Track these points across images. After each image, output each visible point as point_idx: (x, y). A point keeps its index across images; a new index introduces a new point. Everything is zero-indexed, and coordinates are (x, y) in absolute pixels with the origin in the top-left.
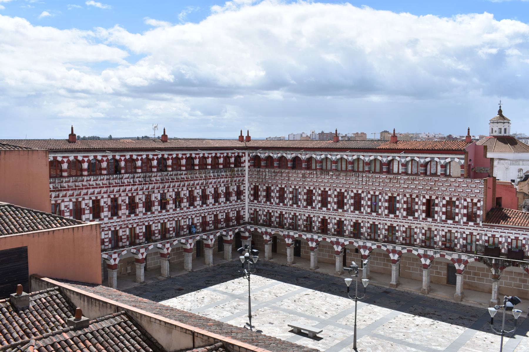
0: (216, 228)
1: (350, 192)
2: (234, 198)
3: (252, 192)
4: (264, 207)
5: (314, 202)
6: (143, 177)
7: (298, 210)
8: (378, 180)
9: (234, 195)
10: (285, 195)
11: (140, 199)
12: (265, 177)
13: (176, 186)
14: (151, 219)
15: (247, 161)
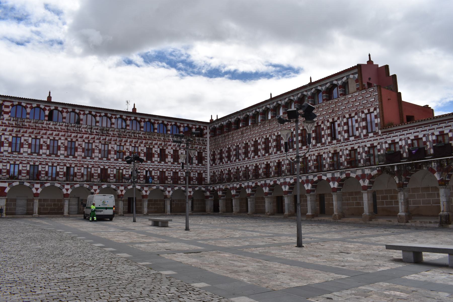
6: (101, 130)
15: (208, 133)
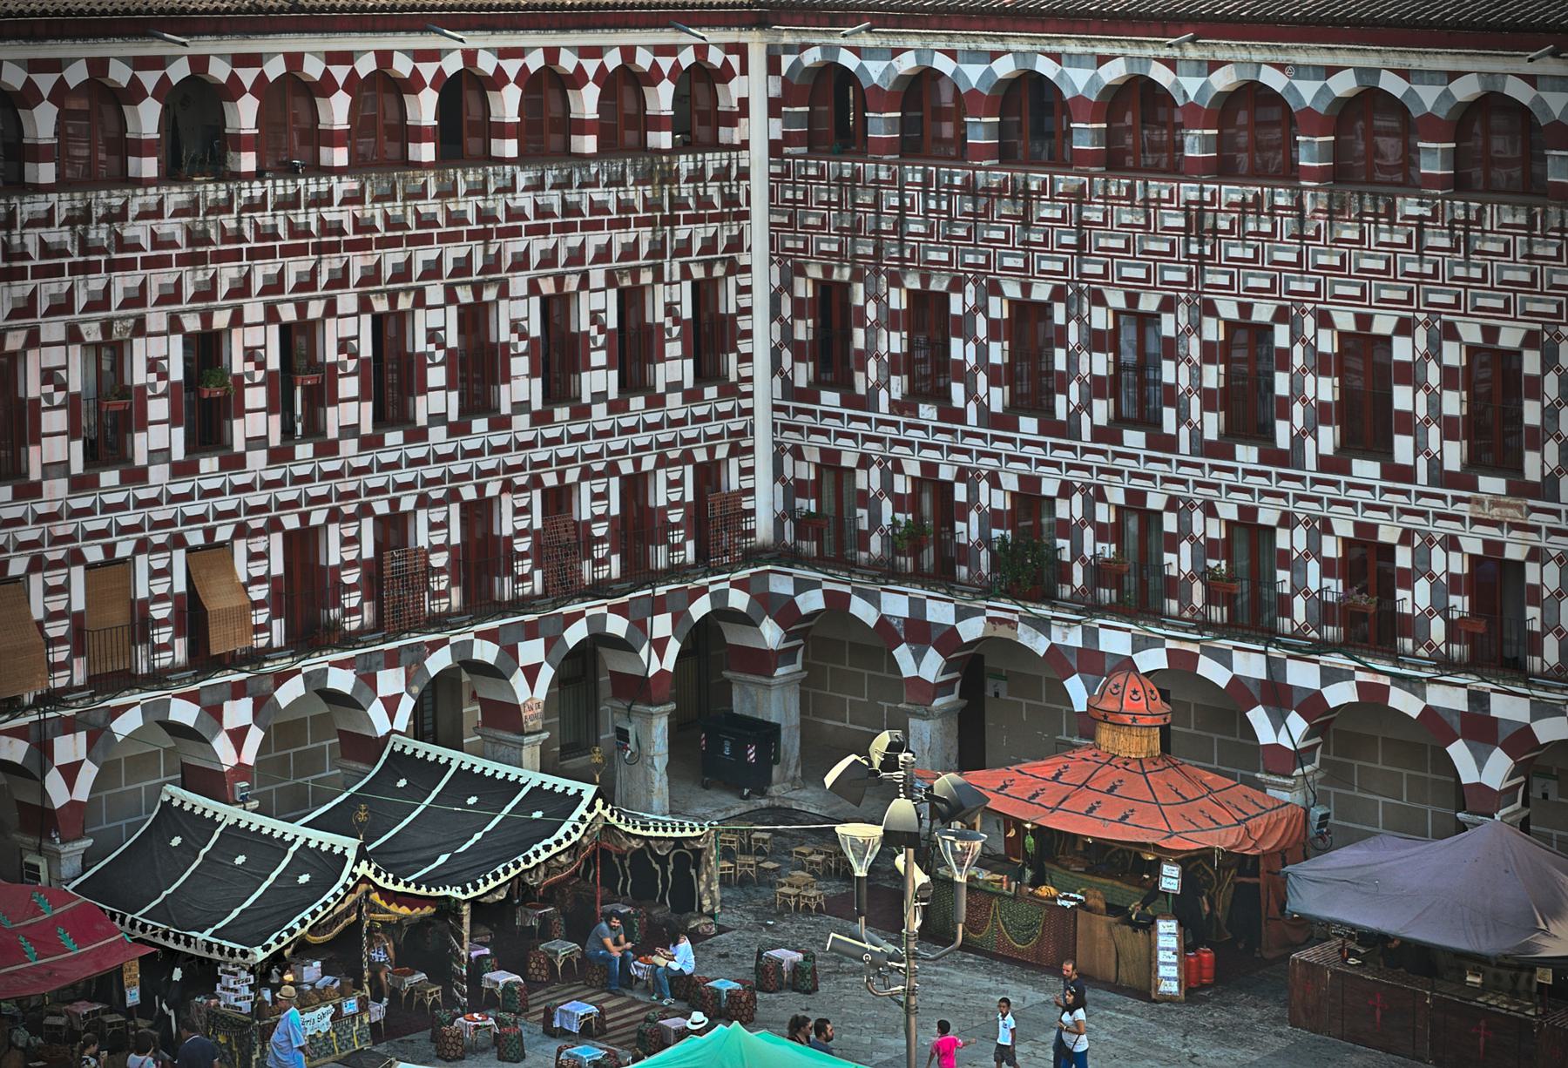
0: (564, 587)
2: (675, 368)
3: (802, 330)
4: (891, 448)
5: (1286, 415)
6: (70, 221)
7: (1159, 469)
9: (673, 348)
11: (48, 376)
12: (901, 222)
13: (290, 281)
14: (127, 519)
15: (758, 108)
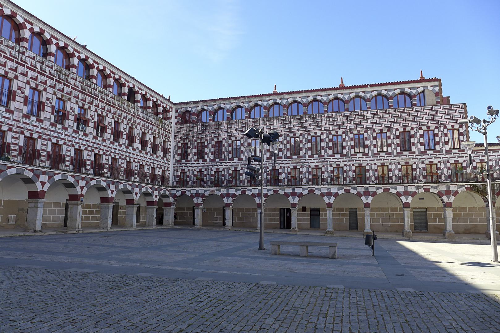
1: (306, 135)
3: (179, 151)
8: (340, 119)
10: (223, 148)
15: (174, 117)
